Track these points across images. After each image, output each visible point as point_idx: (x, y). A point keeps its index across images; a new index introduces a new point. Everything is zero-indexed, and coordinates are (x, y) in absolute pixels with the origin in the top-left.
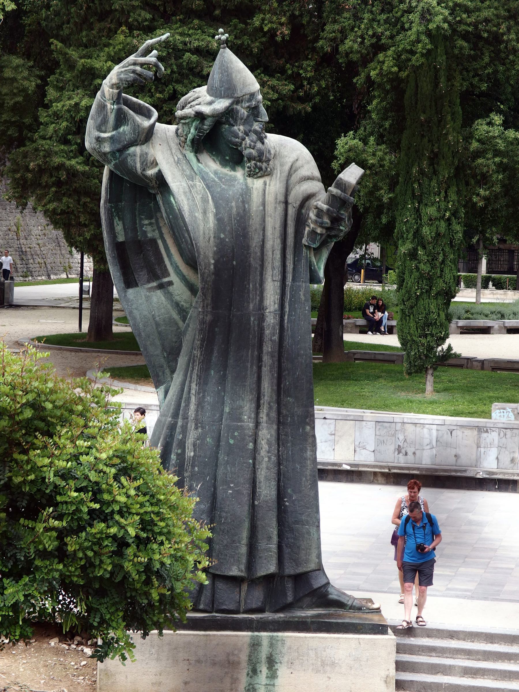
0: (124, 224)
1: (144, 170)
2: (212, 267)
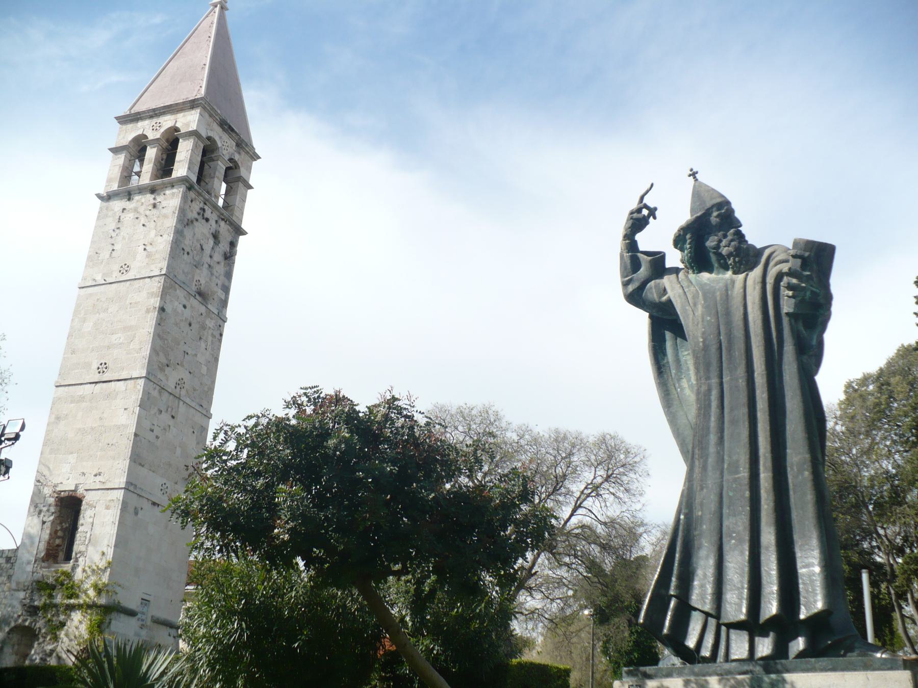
1: (660, 298)
2: (701, 344)
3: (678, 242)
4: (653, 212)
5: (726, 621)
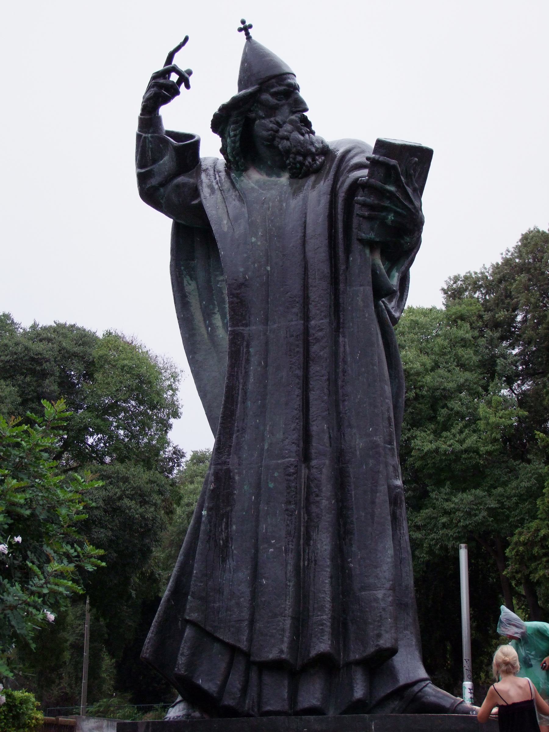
0: (197, 283)
3: (219, 124)
4: (184, 79)
5: (257, 659)
